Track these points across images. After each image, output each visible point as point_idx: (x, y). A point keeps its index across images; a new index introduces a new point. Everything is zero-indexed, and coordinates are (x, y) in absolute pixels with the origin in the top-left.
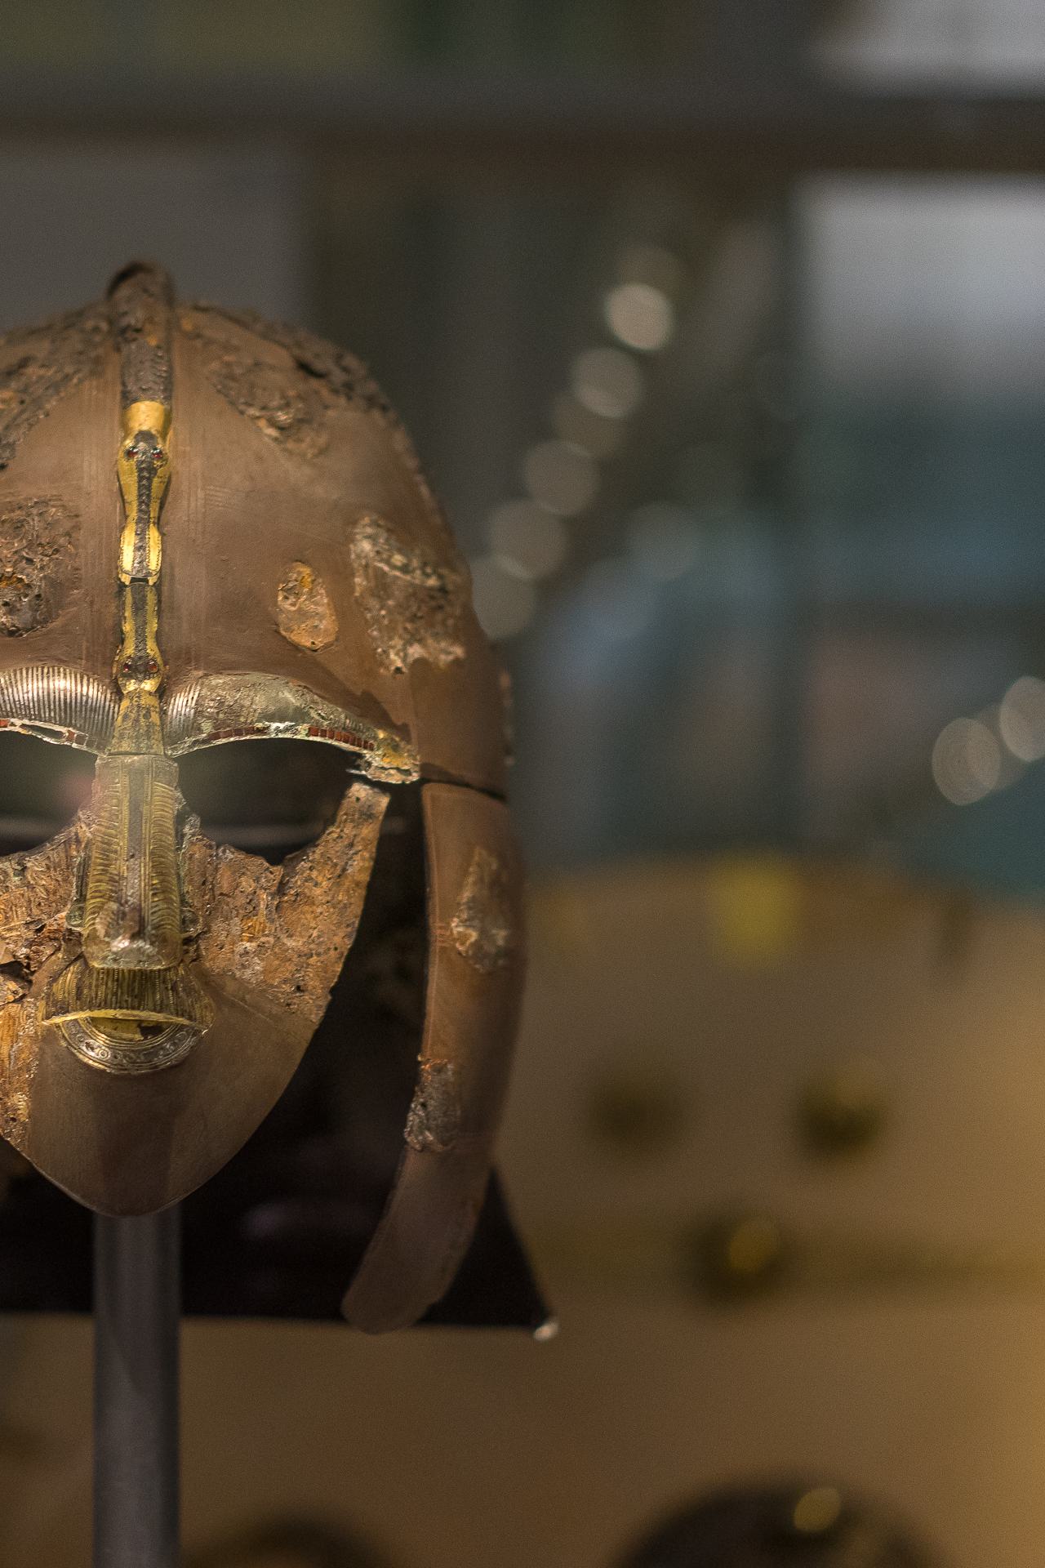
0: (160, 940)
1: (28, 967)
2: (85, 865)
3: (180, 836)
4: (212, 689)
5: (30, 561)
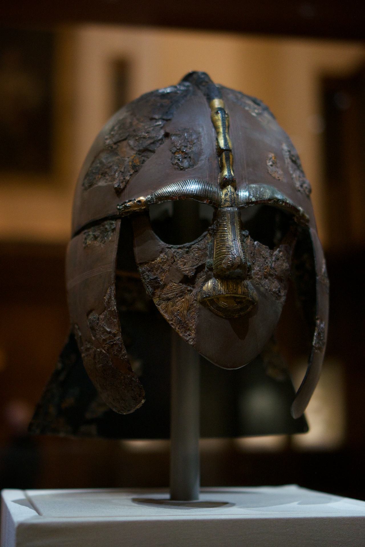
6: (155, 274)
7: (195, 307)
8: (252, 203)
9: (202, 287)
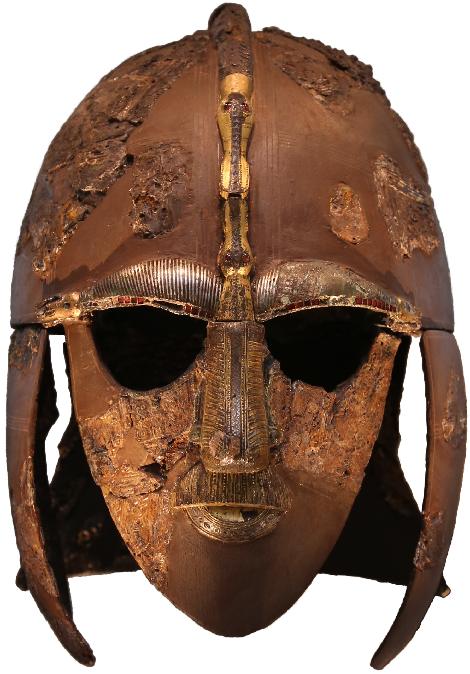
0: (256, 458)
1: (164, 467)
2: (201, 397)
3: (267, 376)
4: (288, 272)
5: (158, 185)
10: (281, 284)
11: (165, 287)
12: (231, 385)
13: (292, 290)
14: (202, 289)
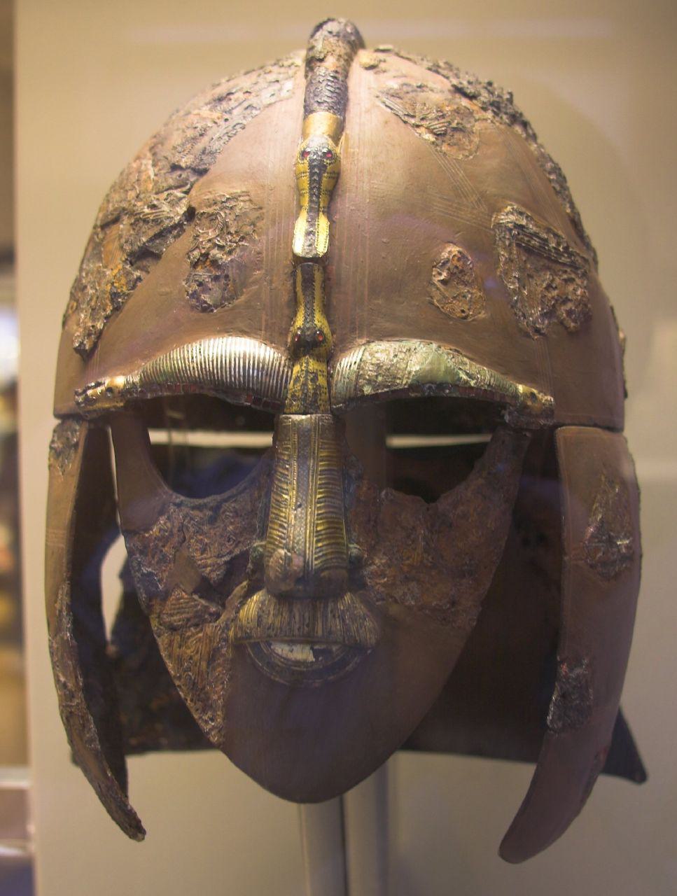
6: (150, 565)
7: (224, 655)
8: (364, 398)
9: (237, 612)
10: (363, 369)
11: (221, 372)
12: (297, 492)
13: (377, 376)
14: (267, 374)
